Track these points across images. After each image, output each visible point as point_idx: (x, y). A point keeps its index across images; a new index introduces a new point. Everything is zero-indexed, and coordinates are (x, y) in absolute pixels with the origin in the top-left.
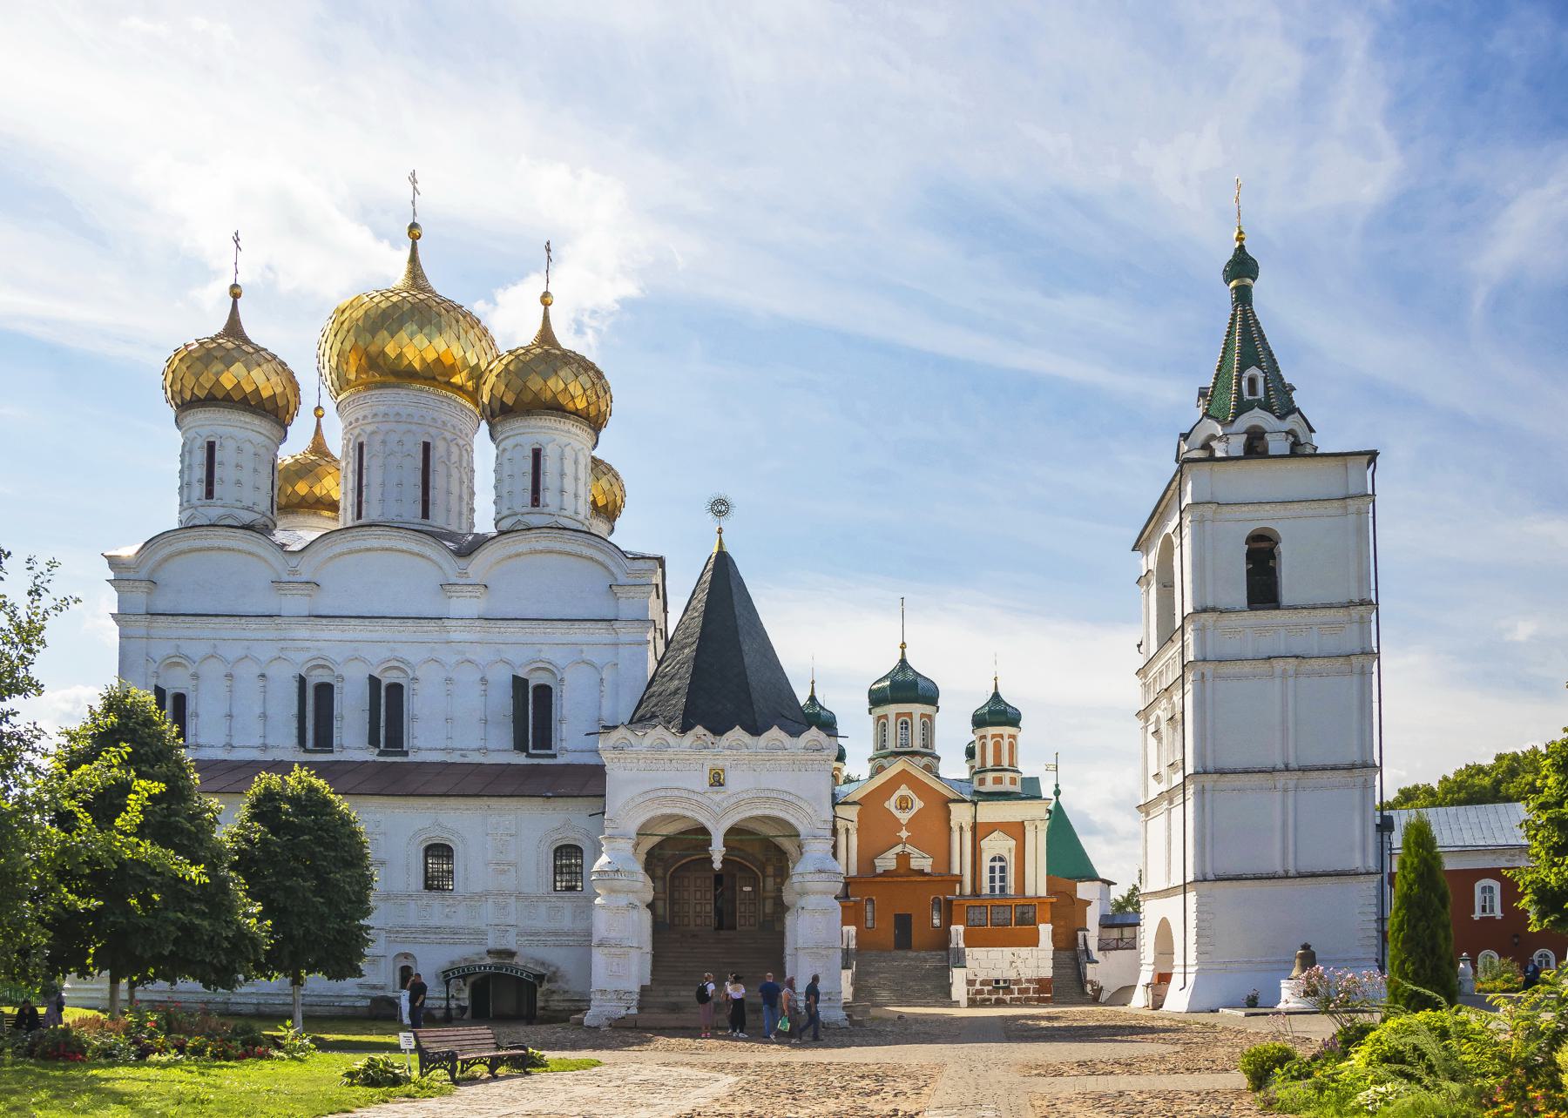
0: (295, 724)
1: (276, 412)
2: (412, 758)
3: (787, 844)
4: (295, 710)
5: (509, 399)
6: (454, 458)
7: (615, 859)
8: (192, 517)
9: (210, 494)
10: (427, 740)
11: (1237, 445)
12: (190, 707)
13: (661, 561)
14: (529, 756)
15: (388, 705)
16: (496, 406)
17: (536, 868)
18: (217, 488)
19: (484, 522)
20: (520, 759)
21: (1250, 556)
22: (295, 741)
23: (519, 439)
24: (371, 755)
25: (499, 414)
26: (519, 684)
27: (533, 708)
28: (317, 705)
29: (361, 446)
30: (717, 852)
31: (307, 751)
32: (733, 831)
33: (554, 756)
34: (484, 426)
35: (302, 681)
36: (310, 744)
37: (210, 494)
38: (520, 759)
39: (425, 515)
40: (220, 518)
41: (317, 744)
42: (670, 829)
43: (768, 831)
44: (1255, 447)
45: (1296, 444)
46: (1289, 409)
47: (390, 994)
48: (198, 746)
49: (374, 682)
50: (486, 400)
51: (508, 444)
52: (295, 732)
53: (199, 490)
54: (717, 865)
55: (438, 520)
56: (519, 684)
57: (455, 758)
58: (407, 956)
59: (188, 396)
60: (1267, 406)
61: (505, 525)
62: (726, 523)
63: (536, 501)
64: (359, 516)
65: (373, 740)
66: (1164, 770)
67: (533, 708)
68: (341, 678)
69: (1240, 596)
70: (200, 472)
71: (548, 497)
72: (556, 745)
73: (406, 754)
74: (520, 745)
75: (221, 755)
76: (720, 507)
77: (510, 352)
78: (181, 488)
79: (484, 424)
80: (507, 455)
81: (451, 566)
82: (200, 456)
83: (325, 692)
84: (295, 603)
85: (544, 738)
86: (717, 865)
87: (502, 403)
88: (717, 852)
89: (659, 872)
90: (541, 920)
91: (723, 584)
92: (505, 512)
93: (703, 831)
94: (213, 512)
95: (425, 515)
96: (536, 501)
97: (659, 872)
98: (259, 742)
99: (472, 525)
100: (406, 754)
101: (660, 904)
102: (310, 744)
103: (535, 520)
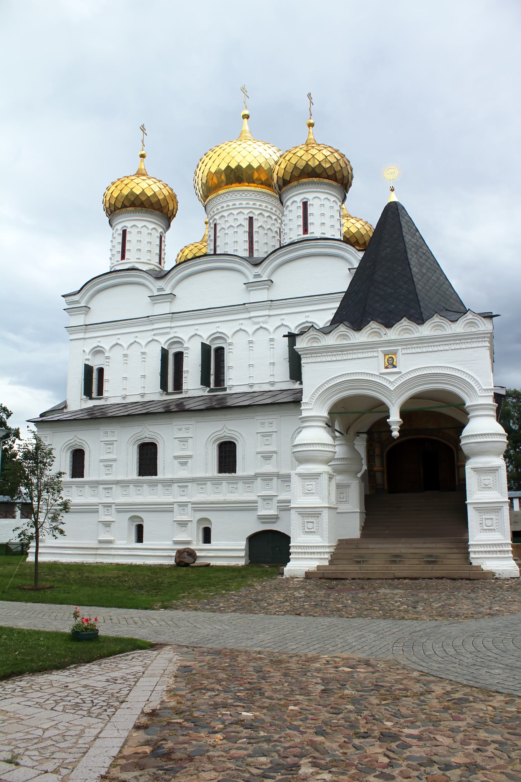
2: (228, 392)
9: (123, 257)
15: (214, 359)
18: (127, 255)
28: (172, 364)
31: (168, 394)
36: (170, 389)
37: (123, 257)
47: (192, 547)
48: (107, 398)
57: (256, 389)
75: (119, 401)
83: (179, 357)
84: (164, 308)
87: (284, 180)
97: (377, 451)
100: (225, 389)
102: (170, 389)
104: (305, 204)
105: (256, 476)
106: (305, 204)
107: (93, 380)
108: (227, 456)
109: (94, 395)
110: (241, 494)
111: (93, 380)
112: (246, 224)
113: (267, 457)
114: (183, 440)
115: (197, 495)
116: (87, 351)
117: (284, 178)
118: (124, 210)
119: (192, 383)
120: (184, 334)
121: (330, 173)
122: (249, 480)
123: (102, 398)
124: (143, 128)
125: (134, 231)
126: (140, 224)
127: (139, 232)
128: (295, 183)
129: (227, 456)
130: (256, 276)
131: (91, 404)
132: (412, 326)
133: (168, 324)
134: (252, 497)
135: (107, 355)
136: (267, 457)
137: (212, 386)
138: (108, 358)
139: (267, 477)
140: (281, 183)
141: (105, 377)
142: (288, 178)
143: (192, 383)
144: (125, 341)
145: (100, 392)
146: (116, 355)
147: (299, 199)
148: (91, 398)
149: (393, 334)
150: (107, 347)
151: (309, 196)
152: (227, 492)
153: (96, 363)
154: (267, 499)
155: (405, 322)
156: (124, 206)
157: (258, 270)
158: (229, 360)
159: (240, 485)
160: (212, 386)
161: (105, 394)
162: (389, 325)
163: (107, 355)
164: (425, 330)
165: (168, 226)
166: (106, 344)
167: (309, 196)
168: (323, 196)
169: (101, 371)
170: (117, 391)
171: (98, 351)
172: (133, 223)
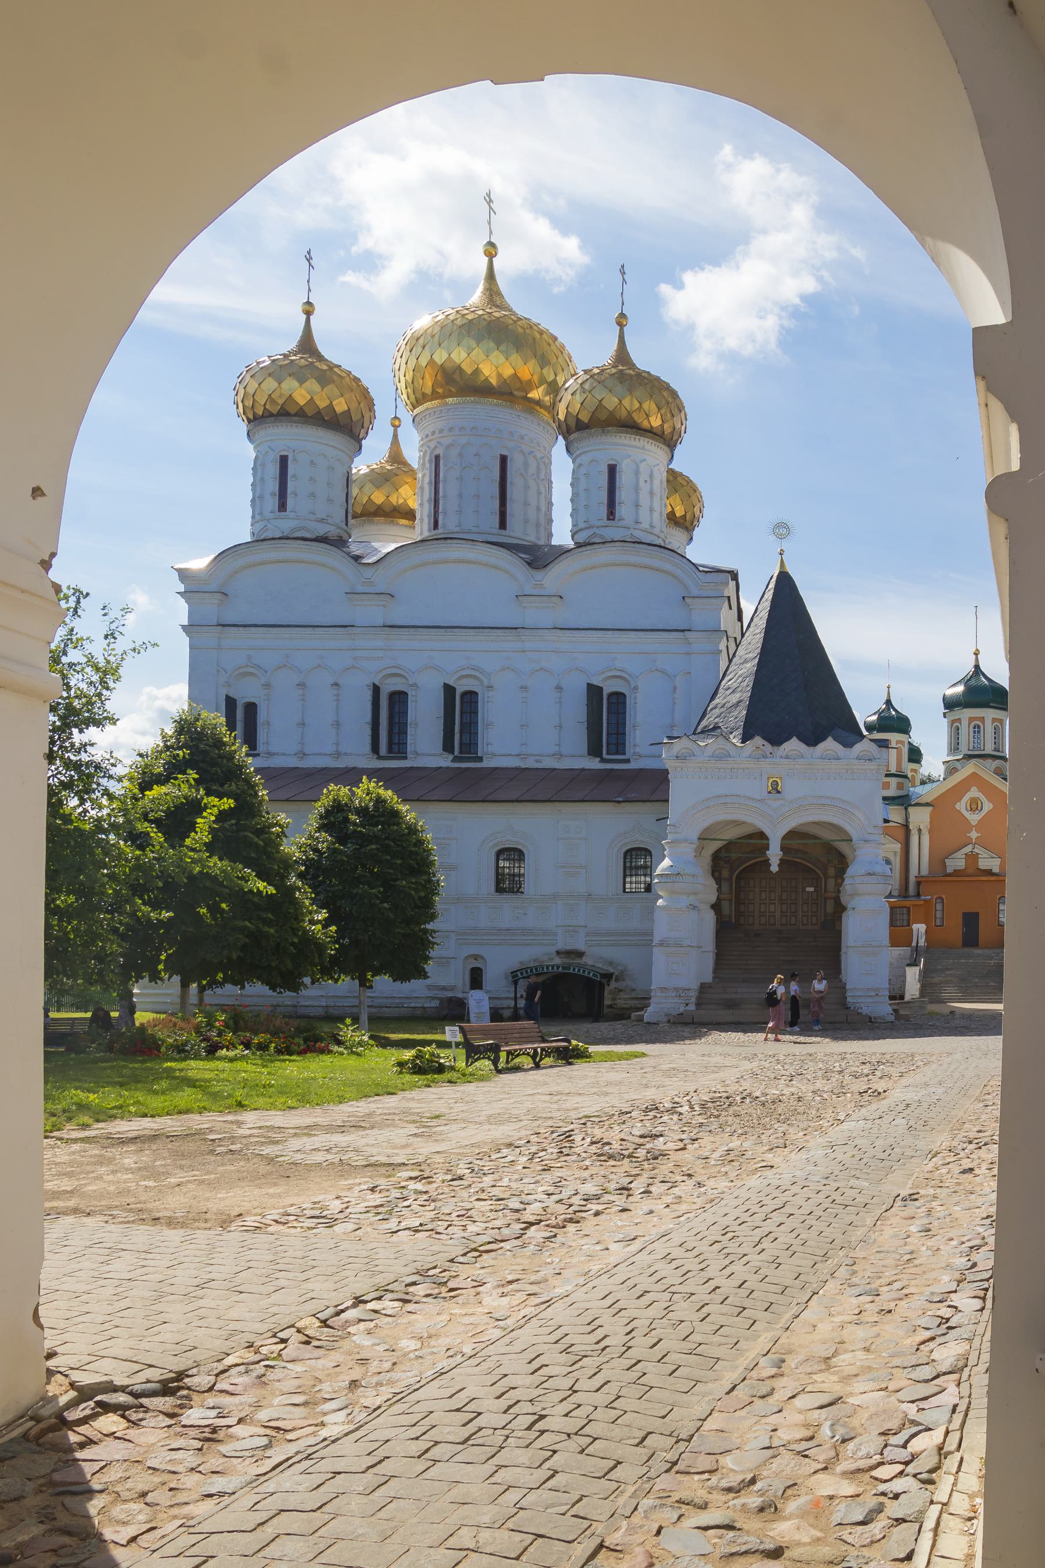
0: (368, 731)
1: (349, 428)
3: (843, 847)
4: (368, 717)
5: (585, 417)
6: (532, 470)
8: (265, 529)
9: (282, 506)
10: (501, 744)
12: (262, 716)
13: (734, 576)
14: (603, 760)
15: (461, 709)
18: (290, 502)
19: (562, 534)
20: (594, 764)
22: (367, 747)
24: (445, 761)
25: (574, 429)
26: (594, 692)
27: (606, 714)
28: (390, 711)
29: (437, 457)
32: (791, 834)
33: (628, 761)
34: (561, 441)
37: (282, 506)
38: (594, 764)
39: (503, 525)
40: (293, 530)
41: (390, 750)
43: (827, 835)
48: (270, 754)
49: (449, 691)
50: (562, 416)
52: (368, 740)
53: (272, 503)
57: (530, 763)
58: (476, 957)
59: (260, 411)
62: (786, 545)
63: (611, 514)
65: (448, 746)
67: (606, 714)
68: (415, 685)
70: (273, 486)
71: (623, 510)
72: (630, 750)
73: (481, 759)
74: (594, 750)
75: (292, 762)
76: (782, 530)
77: (586, 372)
78: (253, 501)
79: (560, 438)
80: (583, 470)
82: (273, 470)
84: (372, 612)
85: (618, 745)
89: (725, 873)
91: (787, 600)
92: (582, 525)
93: (762, 835)
94: (286, 525)
95: (503, 525)
97: (725, 873)
98: (330, 749)
99: (550, 535)
101: (725, 904)
117: (580, 416)
119: (425, 744)
123: (258, 755)
137: (456, 753)
140: (572, 423)
142: (586, 420)
143: (425, 744)
160: (456, 753)
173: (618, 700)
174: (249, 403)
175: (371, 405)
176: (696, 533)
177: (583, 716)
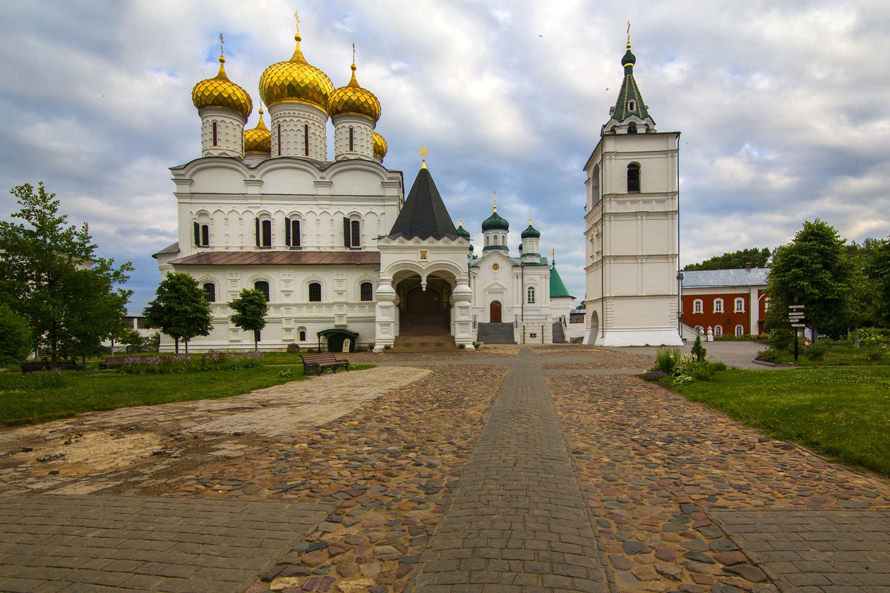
3: (451, 282)
7: (385, 288)
10: (310, 242)
11: (624, 131)
13: (401, 173)
16: (334, 110)
17: (353, 292)
20: (348, 250)
21: (629, 172)
23: (344, 124)
27: (352, 230)
28: (265, 229)
30: (424, 282)
31: (260, 248)
32: (429, 276)
34: (330, 119)
35: (257, 220)
36: (261, 245)
38: (348, 250)
39: (307, 154)
42: (406, 277)
44: (632, 130)
45: (648, 130)
46: (646, 116)
51: (340, 126)
54: (424, 289)
55: (312, 156)
56: (346, 221)
57: (322, 250)
58: (302, 328)
60: (637, 115)
61: (339, 159)
64: (279, 154)
65: (288, 243)
66: (595, 255)
67: (352, 230)
68: (273, 219)
69: (624, 190)
74: (347, 244)
75: (223, 250)
81: (318, 175)
83: (267, 224)
84: (254, 190)
85: (357, 242)
86: (424, 289)
87: (337, 110)
88: (424, 282)
90: (356, 313)
93: (419, 276)
94: (216, 153)
95: (307, 154)
96: (351, 149)
102: (261, 245)
103: (351, 157)
104: (351, 130)
105: (334, 303)
106: (351, 130)
107: (202, 234)
108: (315, 292)
109: (201, 244)
110: (324, 313)
111: (202, 234)
112: (303, 129)
113: (340, 293)
114: (287, 281)
115: (295, 313)
116: (194, 212)
118: (214, 107)
119: (279, 242)
120: (272, 210)
121: (368, 111)
122: (330, 305)
124: (221, 37)
125: (223, 125)
126: (228, 121)
127: (227, 127)
128: (345, 114)
129: (315, 292)
130: (322, 178)
131: (200, 250)
132: (435, 240)
133: (259, 201)
134: (332, 315)
135: (211, 217)
136: (340, 293)
138: (212, 219)
139: (340, 304)
141: (210, 232)
143: (279, 242)
144: (226, 209)
145: (206, 242)
146: (219, 219)
147: (347, 125)
148: (199, 246)
149: (425, 243)
150: (211, 212)
151: (355, 125)
152: (315, 311)
153: (202, 221)
154: (341, 316)
155: (431, 238)
156: (213, 104)
157: (324, 174)
158: (303, 230)
159: (324, 308)
161: (210, 244)
162: (424, 238)
163: (211, 217)
164: (440, 243)
165: (246, 121)
166: (211, 209)
167: (355, 125)
168: (363, 126)
169: (205, 228)
170: (219, 243)
171: (202, 214)
172: (222, 119)
173: (356, 224)
174: (199, 100)
175: (250, 101)
176: (384, 159)
177: (342, 231)
